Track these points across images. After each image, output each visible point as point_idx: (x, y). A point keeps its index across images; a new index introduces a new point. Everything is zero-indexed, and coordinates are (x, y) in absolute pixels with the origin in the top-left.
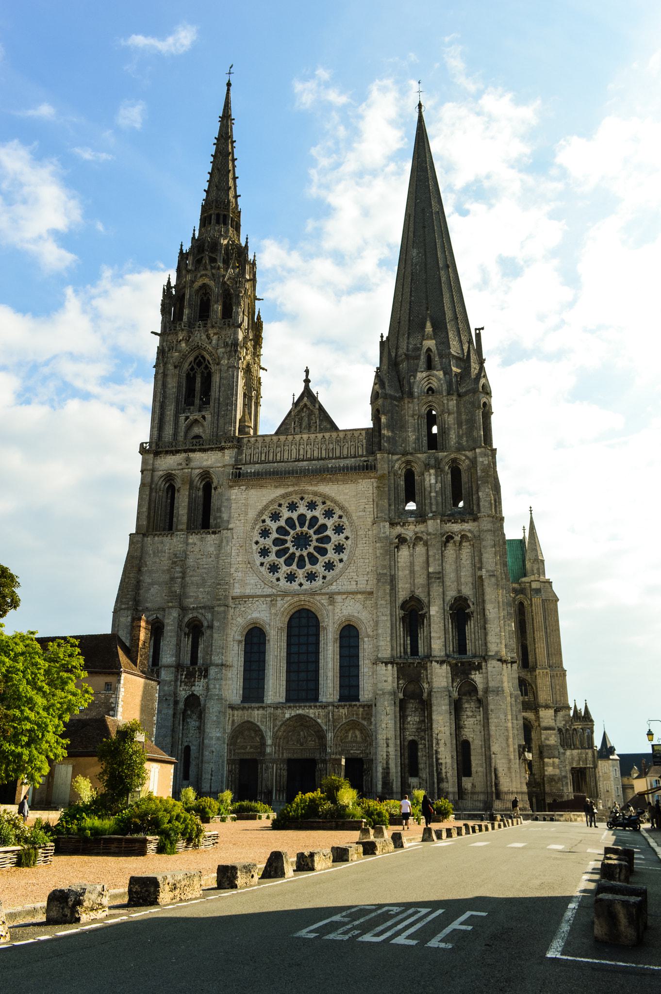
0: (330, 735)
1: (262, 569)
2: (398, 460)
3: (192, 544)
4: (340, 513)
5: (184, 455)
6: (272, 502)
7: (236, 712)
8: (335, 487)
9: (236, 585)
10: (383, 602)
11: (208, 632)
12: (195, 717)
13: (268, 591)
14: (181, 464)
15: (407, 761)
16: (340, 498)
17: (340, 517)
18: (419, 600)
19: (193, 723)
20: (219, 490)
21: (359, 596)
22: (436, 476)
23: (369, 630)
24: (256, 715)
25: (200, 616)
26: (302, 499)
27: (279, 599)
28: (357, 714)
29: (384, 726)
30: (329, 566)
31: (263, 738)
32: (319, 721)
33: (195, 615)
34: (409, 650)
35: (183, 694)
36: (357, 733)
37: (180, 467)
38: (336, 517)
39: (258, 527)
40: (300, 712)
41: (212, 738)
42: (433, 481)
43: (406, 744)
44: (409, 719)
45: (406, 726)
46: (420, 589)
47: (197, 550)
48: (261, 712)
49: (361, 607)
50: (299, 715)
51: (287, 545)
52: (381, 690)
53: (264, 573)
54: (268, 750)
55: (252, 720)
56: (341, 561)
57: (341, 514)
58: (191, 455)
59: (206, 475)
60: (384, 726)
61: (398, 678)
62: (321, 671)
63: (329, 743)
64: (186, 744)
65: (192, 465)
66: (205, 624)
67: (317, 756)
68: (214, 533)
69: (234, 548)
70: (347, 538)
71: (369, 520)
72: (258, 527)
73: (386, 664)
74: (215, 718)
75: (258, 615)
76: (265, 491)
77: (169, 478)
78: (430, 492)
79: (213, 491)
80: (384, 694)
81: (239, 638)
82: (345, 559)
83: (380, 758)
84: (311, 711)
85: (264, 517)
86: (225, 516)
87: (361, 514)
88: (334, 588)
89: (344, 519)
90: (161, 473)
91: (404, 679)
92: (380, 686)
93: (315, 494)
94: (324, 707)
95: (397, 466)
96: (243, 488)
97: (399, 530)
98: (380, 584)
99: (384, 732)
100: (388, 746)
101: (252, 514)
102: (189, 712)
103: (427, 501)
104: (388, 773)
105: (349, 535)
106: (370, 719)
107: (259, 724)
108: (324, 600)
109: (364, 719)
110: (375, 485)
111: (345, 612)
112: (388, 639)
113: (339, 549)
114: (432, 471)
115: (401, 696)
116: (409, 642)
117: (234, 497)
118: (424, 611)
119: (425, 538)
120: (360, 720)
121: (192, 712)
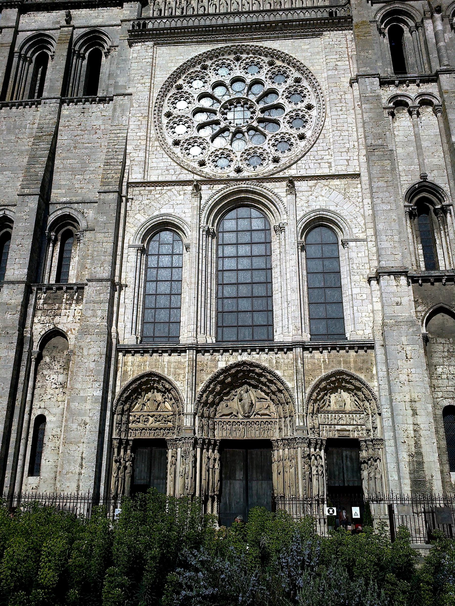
0: (299, 398)
1: (177, 150)
2: (381, 9)
3: (67, 116)
4: (297, 75)
5: (63, 12)
6: (192, 63)
7: (129, 358)
8: (289, 42)
9: (136, 168)
10: (381, 184)
11: (88, 235)
12: (57, 367)
13: (190, 177)
14: (59, 23)
15: (444, 443)
16: (297, 56)
17: (298, 80)
18: (434, 190)
19: (51, 376)
20: (113, 53)
21: (337, 182)
22: (444, 25)
23: (355, 231)
24: (166, 365)
25: (74, 214)
26: (238, 59)
27: (204, 187)
28: (346, 362)
29: (403, 377)
30: (284, 142)
31: (177, 400)
32: (279, 373)
33: (67, 211)
34: (422, 264)
35: (38, 329)
36: (345, 395)
37: (58, 26)
38: (290, 81)
39: (170, 94)
40: (245, 357)
41: (85, 400)
42: (440, 27)
43: (440, 412)
44: (440, 370)
45: (435, 382)
46: (435, 172)
47: (76, 124)
48: (175, 357)
49: (341, 197)
50: (244, 363)
51: (215, 118)
52: (391, 318)
53: (179, 154)
54: (187, 422)
55: (159, 371)
56: (302, 137)
57: (299, 76)
58: (74, 12)
59: (94, 37)
60: (403, 377)
61: (416, 302)
62: (276, 296)
63: (299, 410)
64: (36, 412)
65: (73, 23)
66: (83, 224)
67: (275, 435)
68: (103, 100)
69: (133, 119)
70: (309, 107)
71: (346, 81)
72: (170, 94)
73: (397, 274)
74: (92, 365)
75: (170, 211)
76: (181, 48)
77: (40, 41)
78: (437, 43)
79: (104, 58)
80: (397, 323)
81: (138, 243)
82: (308, 134)
83: (402, 436)
84: (263, 356)
85: (180, 82)
86: (121, 81)
87: (330, 73)
88: (292, 172)
89: (305, 83)
90: (29, 33)
91: (426, 304)
92: (389, 311)
93: (258, 52)
94: (286, 348)
95: (379, 17)
96: (151, 44)
97: (392, 90)
98: (373, 158)
99: (406, 388)
100: (415, 413)
101: (161, 77)
102: (47, 359)
103: (434, 55)
104: (420, 464)
105: (313, 102)
106: (369, 370)
107: (171, 378)
108: (280, 189)
109: (360, 369)
110: (350, 37)
111: (315, 206)
112: (396, 238)
113: (297, 119)
114: (437, 16)
115: (424, 330)
116: (421, 252)
117: (135, 55)
118: (447, 203)
119: (435, 102)
120: (352, 372)
121: (53, 358)
